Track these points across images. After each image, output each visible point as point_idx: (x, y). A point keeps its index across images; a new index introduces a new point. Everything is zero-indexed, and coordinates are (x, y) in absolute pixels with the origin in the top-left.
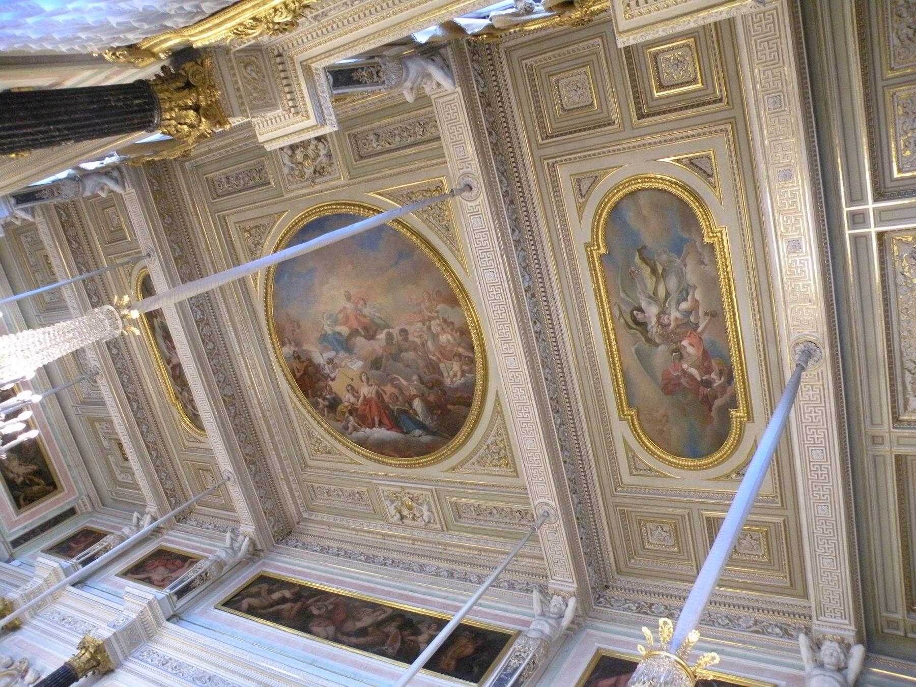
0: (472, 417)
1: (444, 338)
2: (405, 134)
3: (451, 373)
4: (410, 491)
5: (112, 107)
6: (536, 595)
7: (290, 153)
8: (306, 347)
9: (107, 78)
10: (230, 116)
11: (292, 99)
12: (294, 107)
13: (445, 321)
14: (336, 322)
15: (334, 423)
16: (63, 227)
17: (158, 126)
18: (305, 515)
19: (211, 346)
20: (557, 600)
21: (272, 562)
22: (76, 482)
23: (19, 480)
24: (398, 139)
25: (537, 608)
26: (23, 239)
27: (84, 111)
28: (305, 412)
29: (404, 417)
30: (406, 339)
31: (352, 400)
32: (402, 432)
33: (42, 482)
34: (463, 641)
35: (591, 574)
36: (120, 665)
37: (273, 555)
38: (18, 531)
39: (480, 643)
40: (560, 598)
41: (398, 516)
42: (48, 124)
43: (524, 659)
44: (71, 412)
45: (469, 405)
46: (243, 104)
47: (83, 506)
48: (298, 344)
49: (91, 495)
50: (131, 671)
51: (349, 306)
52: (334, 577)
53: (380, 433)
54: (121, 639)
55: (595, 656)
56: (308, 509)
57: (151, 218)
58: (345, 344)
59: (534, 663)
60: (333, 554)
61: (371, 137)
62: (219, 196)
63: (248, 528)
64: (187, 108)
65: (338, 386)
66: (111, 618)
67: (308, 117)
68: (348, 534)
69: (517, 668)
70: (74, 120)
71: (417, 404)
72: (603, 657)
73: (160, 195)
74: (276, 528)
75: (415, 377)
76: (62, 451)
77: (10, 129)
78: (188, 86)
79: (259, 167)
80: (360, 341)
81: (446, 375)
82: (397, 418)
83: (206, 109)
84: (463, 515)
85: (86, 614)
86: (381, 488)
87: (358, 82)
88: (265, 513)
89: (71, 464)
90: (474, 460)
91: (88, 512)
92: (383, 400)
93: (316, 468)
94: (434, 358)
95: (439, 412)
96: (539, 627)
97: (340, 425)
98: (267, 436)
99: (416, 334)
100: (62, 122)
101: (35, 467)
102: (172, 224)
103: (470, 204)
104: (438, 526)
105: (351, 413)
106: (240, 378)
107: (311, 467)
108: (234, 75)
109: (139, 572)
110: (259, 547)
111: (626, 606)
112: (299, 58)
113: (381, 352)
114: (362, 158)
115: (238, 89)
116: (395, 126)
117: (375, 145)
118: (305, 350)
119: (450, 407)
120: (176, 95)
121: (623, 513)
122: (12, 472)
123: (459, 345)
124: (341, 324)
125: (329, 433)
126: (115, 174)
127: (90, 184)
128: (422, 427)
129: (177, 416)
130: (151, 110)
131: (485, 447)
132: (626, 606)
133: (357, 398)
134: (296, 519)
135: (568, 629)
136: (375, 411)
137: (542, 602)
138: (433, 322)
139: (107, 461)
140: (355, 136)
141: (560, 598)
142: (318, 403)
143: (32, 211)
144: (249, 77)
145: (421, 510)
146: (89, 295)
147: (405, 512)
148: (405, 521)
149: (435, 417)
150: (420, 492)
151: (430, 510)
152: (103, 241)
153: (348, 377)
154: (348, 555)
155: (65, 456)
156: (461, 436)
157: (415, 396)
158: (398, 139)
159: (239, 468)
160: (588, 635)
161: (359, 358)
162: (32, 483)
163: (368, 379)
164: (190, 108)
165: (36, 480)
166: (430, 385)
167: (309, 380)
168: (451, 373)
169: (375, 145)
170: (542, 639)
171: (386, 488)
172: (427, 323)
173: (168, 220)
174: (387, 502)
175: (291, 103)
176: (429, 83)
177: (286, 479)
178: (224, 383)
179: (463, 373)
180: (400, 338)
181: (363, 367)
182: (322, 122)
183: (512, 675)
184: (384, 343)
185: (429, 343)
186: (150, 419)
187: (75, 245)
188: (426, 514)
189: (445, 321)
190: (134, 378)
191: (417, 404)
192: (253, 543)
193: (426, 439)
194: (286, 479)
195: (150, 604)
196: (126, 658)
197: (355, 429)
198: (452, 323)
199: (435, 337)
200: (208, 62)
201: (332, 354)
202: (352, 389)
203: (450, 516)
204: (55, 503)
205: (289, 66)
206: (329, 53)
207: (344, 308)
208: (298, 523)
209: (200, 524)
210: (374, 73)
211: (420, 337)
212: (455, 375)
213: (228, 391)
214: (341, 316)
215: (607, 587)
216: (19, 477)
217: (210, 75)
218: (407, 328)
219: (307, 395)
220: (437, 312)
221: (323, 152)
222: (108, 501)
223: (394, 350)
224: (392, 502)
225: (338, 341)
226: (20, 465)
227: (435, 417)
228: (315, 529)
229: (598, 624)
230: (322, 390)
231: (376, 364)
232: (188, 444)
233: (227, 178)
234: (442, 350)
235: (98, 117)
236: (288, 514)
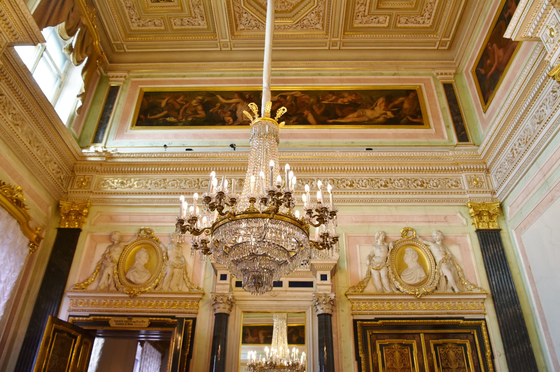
26: (134, 27)
33: (401, 99)
76: (376, 74)
89: (393, 72)
91: (455, 74)
101: (381, 100)
122: (378, 118)
155: (382, 74)
162: (400, 106)
165: (397, 102)
204: (431, 96)
216: (386, 114)
226: (373, 109)
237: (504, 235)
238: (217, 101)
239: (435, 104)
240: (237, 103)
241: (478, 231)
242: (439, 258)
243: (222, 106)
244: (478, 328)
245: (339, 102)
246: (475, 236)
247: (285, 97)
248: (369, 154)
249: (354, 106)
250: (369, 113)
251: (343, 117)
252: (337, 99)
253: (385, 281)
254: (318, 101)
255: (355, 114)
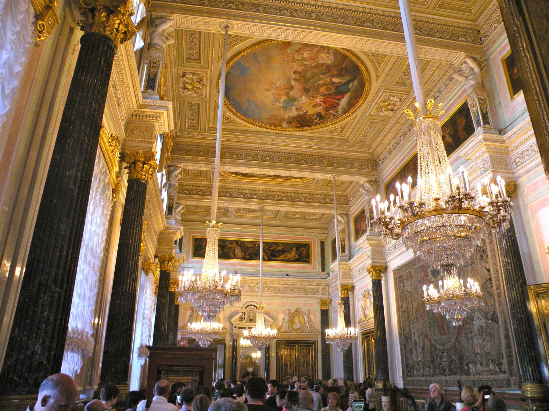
0: (354, 58)
1: (306, 55)
2: (194, 36)
3: (326, 59)
4: (380, 100)
5: (134, 198)
6: (456, 76)
7: (186, 90)
8: (286, 117)
9: (123, 193)
10: (151, 150)
11: (153, 117)
12: (156, 117)
13: (297, 52)
14: (278, 100)
15: (329, 120)
16: (191, 194)
17: (147, 181)
18: (371, 151)
19: (268, 159)
20: (464, 66)
21: (385, 176)
22: (310, 235)
23: (297, 257)
24: (195, 40)
25: (462, 79)
26: (192, 210)
27: (133, 209)
28: (318, 130)
29: (340, 88)
30: (300, 73)
31: (321, 107)
32: (348, 92)
34: (459, 121)
35: (464, 39)
36: (386, 263)
37: (381, 175)
38: (319, 268)
39: (464, 114)
40: (464, 64)
41: (390, 111)
42: (134, 224)
43: (476, 104)
44: (277, 223)
45: (346, 57)
46: (148, 142)
47: (322, 237)
48: (283, 120)
49: (320, 232)
50: (392, 260)
51: (272, 91)
52: (403, 156)
53: (344, 102)
54: (376, 257)
55: (502, 62)
56: (369, 148)
57: (197, 161)
58: (291, 100)
59: (482, 100)
60: (394, 149)
61: (191, 51)
62: (198, 126)
63: (362, 180)
64: (143, 167)
65: (312, 111)
66: (366, 257)
67: (163, 113)
68: (389, 137)
69: (478, 110)
70: (135, 214)
71: (335, 80)
72: (506, 60)
73: (188, 152)
74: (370, 167)
75: (321, 76)
77: (132, 237)
78: (134, 163)
79: (190, 105)
80: (292, 93)
81: (325, 62)
82: (340, 91)
83: (146, 159)
84: (405, 82)
85: (362, 262)
86: (372, 113)
87: (155, 76)
88: (360, 169)
90: (377, 65)
92: (327, 94)
93: (349, 136)
94: (314, 64)
95: (344, 72)
96: (469, 86)
97: (332, 117)
98: (323, 151)
99: (299, 67)
100: (135, 218)
101: (294, 249)
102: (204, 152)
103: (236, 29)
104: (404, 96)
105: (327, 111)
106: (289, 151)
107: (348, 138)
108: (135, 141)
109: (359, 233)
110: (374, 179)
111: (493, 28)
112: (136, 108)
113: (302, 87)
114: (199, 59)
115: (142, 141)
116: (188, 40)
117: (195, 51)
118: (288, 118)
119: (343, 66)
120: (137, 170)
121: (441, 6)
123: (312, 50)
124: (280, 98)
125: (334, 124)
126: (172, 168)
127: (173, 182)
128: (348, 82)
129: (298, 183)
130: (140, 183)
131: (373, 57)
132: (493, 28)
133: (321, 105)
134: (371, 156)
135: (481, 70)
136: (331, 100)
137: (461, 75)
138: (295, 57)
139: (308, 219)
140: (188, 58)
141: (464, 64)
142: (317, 122)
143: (179, 204)
144: (138, 133)
145: (392, 100)
146: (225, 197)
147: (390, 107)
148: (395, 109)
149: (346, 74)
150: (382, 97)
151: (394, 96)
152: (202, 180)
153: (308, 105)
154: (397, 143)
156: (362, 68)
157: (331, 79)
158: (195, 40)
159: (331, 171)
160: (494, 58)
161: (301, 97)
163: (313, 97)
164: (143, 165)
166: (328, 71)
167: (303, 122)
168: (326, 59)
169: (195, 51)
170: (474, 89)
171: (373, 110)
172: (295, 60)
173: (202, 153)
174: (381, 114)
175: (154, 119)
176: (167, 31)
177: (348, 151)
178: (288, 160)
179: (328, 53)
180: (298, 75)
181: (306, 96)
182: (166, 108)
183: (478, 115)
184: (297, 83)
185: (305, 63)
186: (294, 195)
187: (201, 193)
188: (395, 99)
189: (297, 52)
190: (272, 193)
191: (335, 80)
192: (370, 182)
193: (356, 83)
194: (348, 151)
195: (368, 240)
196: (385, 259)
197: (337, 112)
198: (299, 49)
199: (304, 59)
200: (127, 151)
201: (294, 108)
202: (316, 106)
203: (402, 88)
204: (315, 247)
205: (138, 113)
206: (136, 96)
207: (273, 94)
208: (373, 156)
209: (353, 196)
210: (154, 64)
211: (301, 66)
212: (328, 57)
213: (293, 159)
214: (276, 97)
215: (479, 31)
217: (132, 152)
218: (294, 70)
219: (309, 126)
220: (291, 53)
221: (191, 76)
222: (326, 226)
223: (303, 80)
224: (382, 111)
225: (288, 103)
227: (346, 74)
228: (379, 150)
229: (492, 50)
230: (310, 119)
231: (306, 91)
232: (313, 184)
233: (191, 119)
234: (311, 59)
235: (137, 205)
236: (366, 158)
237: (330, 311)
238: (227, 245)
239: (315, 252)
240: (235, 247)
241: (321, 310)
242: (306, 320)
243: (229, 249)
244: (314, 343)
245: (277, 249)
246: (320, 312)
247: (255, 245)
248: (288, 279)
249: (283, 251)
250: (289, 256)
251: (279, 257)
252: (277, 247)
253: (287, 328)
254: (269, 248)
255: (283, 256)
